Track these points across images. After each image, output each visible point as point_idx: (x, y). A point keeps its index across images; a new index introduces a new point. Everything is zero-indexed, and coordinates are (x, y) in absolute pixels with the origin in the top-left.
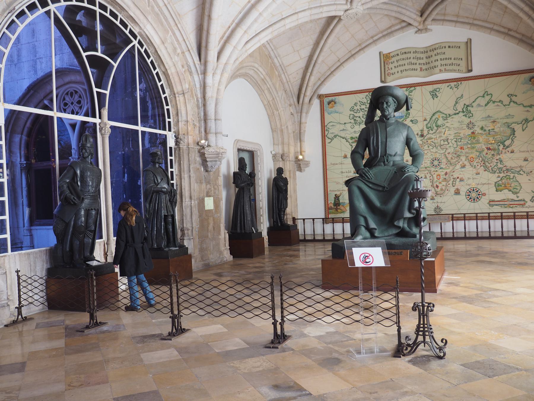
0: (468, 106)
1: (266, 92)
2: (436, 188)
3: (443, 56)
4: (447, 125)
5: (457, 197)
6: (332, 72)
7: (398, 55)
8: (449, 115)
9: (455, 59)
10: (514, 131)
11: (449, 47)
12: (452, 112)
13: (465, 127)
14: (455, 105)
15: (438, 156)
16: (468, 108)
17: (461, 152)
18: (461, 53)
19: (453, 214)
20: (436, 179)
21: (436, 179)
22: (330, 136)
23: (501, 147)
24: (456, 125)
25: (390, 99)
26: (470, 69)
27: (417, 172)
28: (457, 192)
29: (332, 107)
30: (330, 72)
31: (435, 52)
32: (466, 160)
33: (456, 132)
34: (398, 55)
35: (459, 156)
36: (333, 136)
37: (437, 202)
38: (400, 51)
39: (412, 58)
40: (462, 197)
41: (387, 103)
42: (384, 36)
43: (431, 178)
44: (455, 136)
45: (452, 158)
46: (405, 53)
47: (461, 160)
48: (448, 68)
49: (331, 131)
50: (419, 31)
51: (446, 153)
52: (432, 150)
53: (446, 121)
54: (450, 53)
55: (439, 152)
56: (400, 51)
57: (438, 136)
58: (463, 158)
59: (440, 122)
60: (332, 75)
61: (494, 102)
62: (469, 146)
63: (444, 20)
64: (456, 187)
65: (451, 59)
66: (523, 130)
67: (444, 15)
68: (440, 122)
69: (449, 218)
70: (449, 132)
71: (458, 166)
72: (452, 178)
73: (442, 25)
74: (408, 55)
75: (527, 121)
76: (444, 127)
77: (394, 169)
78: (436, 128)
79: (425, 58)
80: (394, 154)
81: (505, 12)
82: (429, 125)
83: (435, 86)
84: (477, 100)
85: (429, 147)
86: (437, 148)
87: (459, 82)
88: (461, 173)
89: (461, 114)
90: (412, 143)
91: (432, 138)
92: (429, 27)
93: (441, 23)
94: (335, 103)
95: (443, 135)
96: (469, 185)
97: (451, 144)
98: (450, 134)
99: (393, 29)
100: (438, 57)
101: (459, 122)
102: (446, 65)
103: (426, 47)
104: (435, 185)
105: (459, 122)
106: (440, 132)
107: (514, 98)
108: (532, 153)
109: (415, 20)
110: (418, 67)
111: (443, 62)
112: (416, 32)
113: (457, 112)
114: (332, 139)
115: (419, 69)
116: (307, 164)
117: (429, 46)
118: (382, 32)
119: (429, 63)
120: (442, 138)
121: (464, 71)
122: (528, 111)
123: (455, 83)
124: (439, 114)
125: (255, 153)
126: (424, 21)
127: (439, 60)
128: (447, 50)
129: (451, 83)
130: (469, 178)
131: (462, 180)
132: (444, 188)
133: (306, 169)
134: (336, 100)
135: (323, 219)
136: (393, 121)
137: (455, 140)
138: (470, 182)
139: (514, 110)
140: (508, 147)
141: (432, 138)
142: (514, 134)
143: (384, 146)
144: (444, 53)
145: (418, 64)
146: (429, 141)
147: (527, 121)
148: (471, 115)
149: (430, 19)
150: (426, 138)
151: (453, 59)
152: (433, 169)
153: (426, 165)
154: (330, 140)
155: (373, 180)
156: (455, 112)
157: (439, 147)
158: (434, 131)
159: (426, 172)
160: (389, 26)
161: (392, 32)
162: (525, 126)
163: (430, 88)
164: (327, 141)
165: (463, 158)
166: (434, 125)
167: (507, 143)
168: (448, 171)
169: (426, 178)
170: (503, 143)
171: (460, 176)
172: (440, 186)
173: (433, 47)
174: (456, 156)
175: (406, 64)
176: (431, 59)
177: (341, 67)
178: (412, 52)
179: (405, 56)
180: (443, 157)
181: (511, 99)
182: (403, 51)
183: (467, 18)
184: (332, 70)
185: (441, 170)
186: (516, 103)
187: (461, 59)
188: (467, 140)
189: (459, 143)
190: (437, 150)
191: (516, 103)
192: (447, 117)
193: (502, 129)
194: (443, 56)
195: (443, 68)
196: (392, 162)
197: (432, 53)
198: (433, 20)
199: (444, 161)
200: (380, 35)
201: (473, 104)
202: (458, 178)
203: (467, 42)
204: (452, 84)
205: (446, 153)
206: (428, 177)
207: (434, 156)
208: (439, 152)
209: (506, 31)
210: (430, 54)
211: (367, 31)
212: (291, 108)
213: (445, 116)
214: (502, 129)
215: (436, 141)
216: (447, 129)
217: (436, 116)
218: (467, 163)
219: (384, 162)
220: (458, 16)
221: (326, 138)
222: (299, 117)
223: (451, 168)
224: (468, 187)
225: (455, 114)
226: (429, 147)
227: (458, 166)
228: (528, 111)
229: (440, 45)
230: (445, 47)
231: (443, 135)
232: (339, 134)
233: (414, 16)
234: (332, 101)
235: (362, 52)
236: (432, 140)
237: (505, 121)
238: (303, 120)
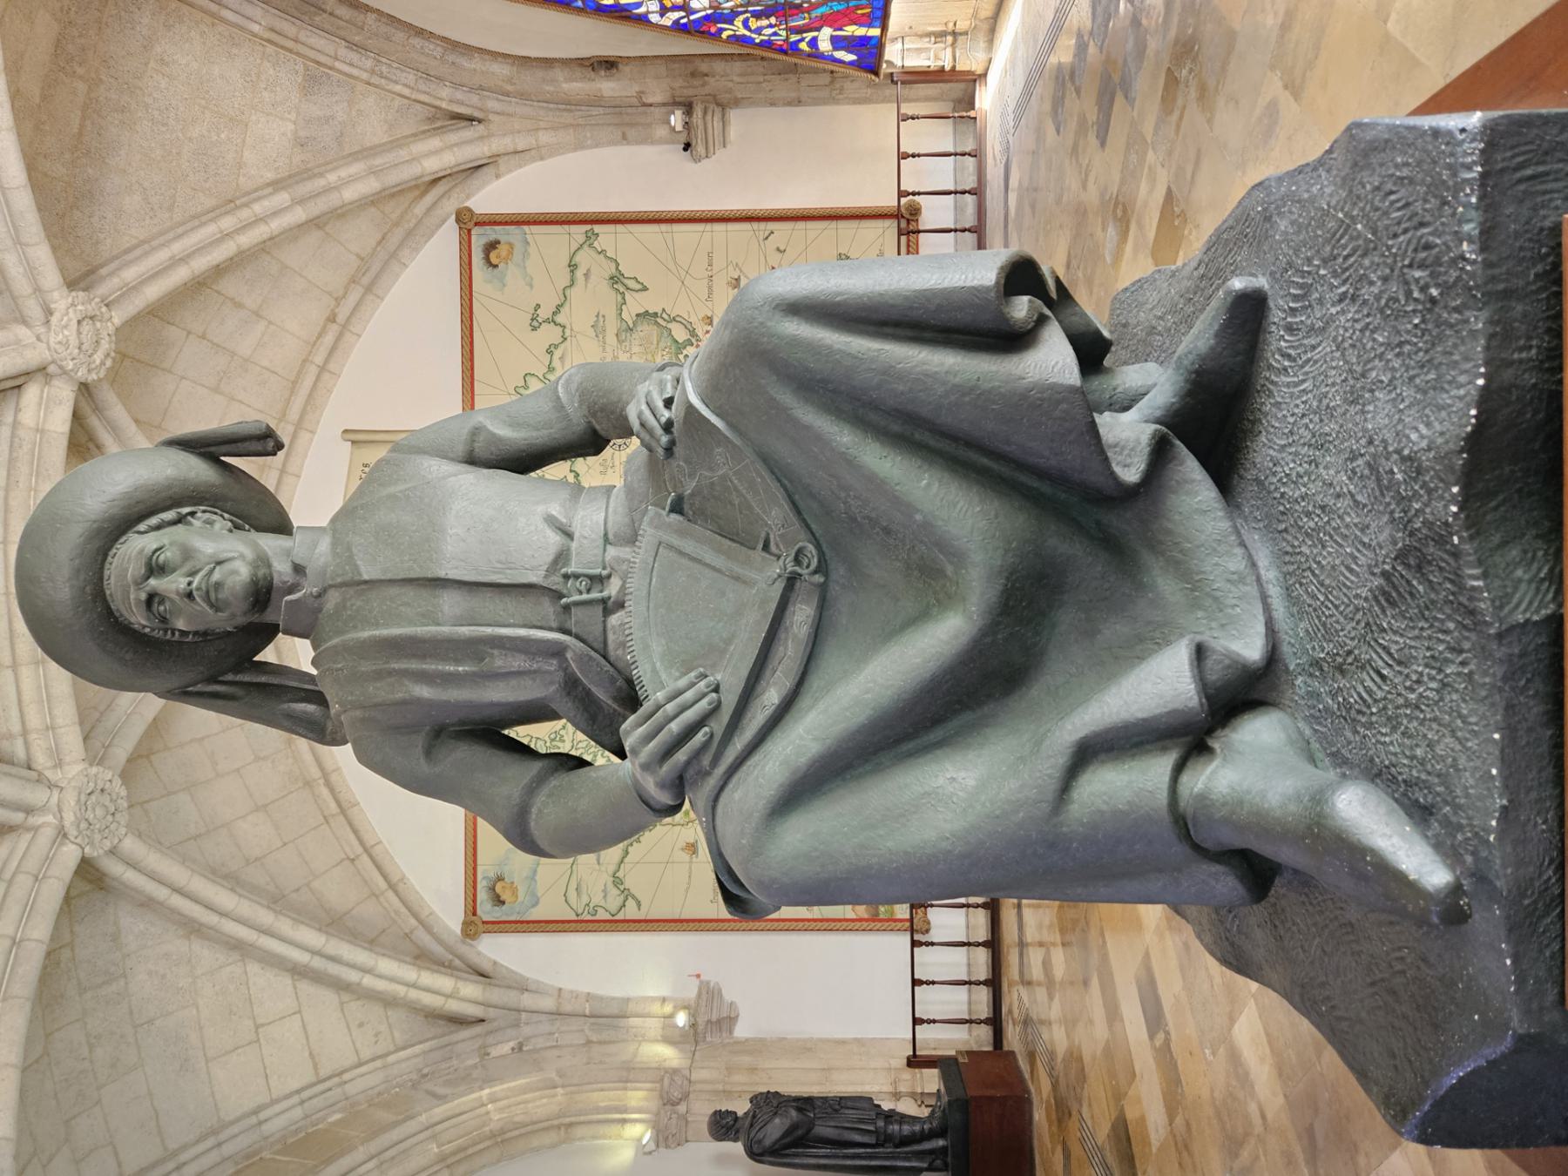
6: (392, 887)
10: (644, 315)
22: (613, 902)
23: (690, 351)
29: (514, 892)
30: (390, 894)
36: (616, 892)
49: (597, 899)
60: (401, 887)
61: (551, 369)
66: (645, 289)
75: (616, 279)
80: (554, 539)
81: (257, 314)
94: (500, 879)
107: (544, 313)
108: (715, 268)
114: (627, 894)
116: (709, 993)
122: (587, 275)
133: (729, 995)
134: (492, 875)
135: (914, 944)
139: (579, 315)
140: (693, 333)
142: (656, 314)
147: (616, 279)
154: (631, 903)
162: (632, 284)
164: (631, 912)
167: (680, 334)
170: (680, 347)
177: (377, 851)
181: (547, 321)
184: (383, 884)
186: (559, 308)
191: (559, 308)
193: (636, 349)
203: (353, 442)
209: (334, 330)
211: (258, 759)
212: (495, 1052)
214: (636, 349)
221: (620, 916)
222: (535, 1017)
228: (587, 275)
232: (612, 868)
234: (492, 889)
235: (334, 778)
237: (611, 338)
238: (548, 1003)
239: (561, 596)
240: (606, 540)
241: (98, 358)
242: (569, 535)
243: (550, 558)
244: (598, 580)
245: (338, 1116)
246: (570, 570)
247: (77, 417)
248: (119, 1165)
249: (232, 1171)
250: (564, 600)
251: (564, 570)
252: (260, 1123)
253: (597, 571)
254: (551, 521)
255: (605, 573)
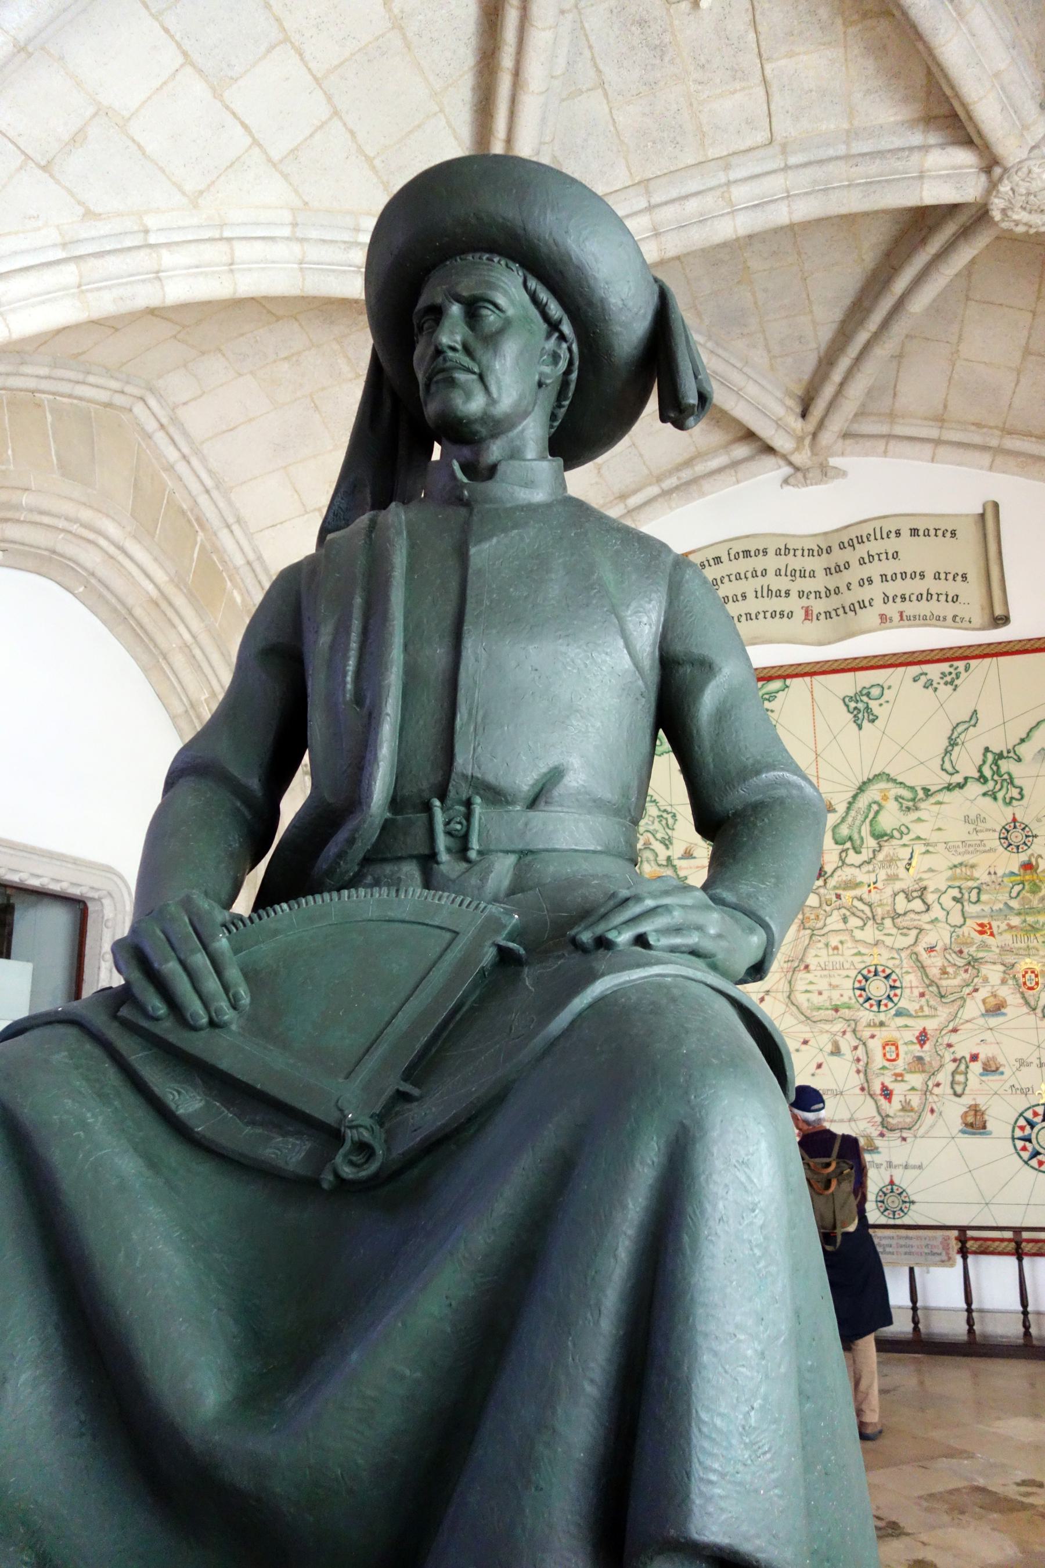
0: (1000, 756)
1: (179, 660)
2: (882, 1101)
3: (890, 567)
4: (917, 830)
5: (973, 1143)
7: (718, 560)
8: (926, 790)
9: (937, 576)
11: (914, 532)
12: (938, 780)
13: (992, 840)
14: (946, 752)
15: (882, 958)
16: (1005, 765)
17: (984, 946)
18: (963, 554)
19: (962, 1229)
20: (878, 1061)
21: (878, 1061)
24: (958, 832)
25: (510, 290)
26: (999, 611)
27: (757, 971)
28: (975, 1123)
31: (862, 550)
32: (1004, 982)
33: (957, 860)
34: (718, 560)
35: (973, 963)
37: (890, 1165)
38: (727, 546)
39: (771, 572)
40: (997, 1146)
41: (473, 308)
42: (666, 494)
43: (860, 1052)
44: (953, 878)
45: (944, 972)
46: (747, 553)
47: (986, 980)
48: (911, 608)
50: (799, 474)
51: (920, 949)
52: (859, 934)
53: (914, 815)
54: (916, 554)
55: (889, 940)
56: (727, 546)
57: (882, 875)
58: (993, 973)
59: (889, 819)
62: (1015, 921)
63: (889, 437)
64: (967, 1100)
65: (922, 576)
67: (892, 416)
68: (889, 819)
69: (946, 1248)
70: (929, 861)
71: (973, 1008)
72: (948, 1056)
73: (885, 453)
74: (757, 563)
76: (906, 839)
77: (493, 924)
78: (872, 843)
79: (820, 573)
80: (525, 781)
82: (844, 831)
83: (866, 678)
84: (1037, 734)
85: (845, 920)
86: (880, 926)
87: (961, 664)
88: (988, 1035)
89: (975, 789)
90: (708, 702)
91: (858, 885)
92: (833, 461)
93: (881, 444)
95: (902, 872)
96: (1025, 1092)
97: (936, 912)
98: (933, 869)
99: (700, 468)
100: (874, 570)
101: (967, 819)
102: (903, 598)
103: (826, 534)
104: (877, 1088)
105: (967, 819)
106: (891, 861)
109: (778, 424)
110: (793, 603)
111: (894, 588)
112: (786, 481)
113: (958, 779)
115: (800, 614)
117: (837, 530)
118: (659, 480)
119: (837, 591)
120: (898, 886)
121: (978, 619)
123: (945, 667)
124: (882, 785)
125: (91, 907)
126: (815, 435)
127: (876, 579)
128: (905, 544)
129: (925, 668)
130: (1022, 1063)
131: (991, 1069)
132: (915, 1101)
136: (539, 496)
137: (955, 893)
138: (1027, 1077)
141: (858, 885)
143: (430, 702)
144: (896, 555)
145: (794, 594)
146: (847, 895)
148: (1015, 793)
149: (837, 424)
150: (832, 882)
151: (929, 575)
152: (865, 1016)
153: (835, 994)
155: (233, 1051)
156: (947, 779)
157: (888, 922)
158: (866, 854)
159: (839, 1026)
160: (686, 456)
161: (695, 481)
163: (846, 683)
165: (993, 973)
166: (865, 830)
168: (931, 1025)
169: (836, 1051)
171: (984, 1053)
172: (899, 1090)
173: (853, 533)
174: (960, 962)
175: (751, 595)
176: (847, 576)
178: (771, 552)
179: (744, 565)
180: (907, 964)
182: (739, 547)
183: (978, 425)
185: (900, 1021)
187: (964, 577)
188: (1004, 897)
189: (971, 909)
190: (879, 936)
192: (915, 799)
194: (890, 567)
195: (892, 610)
196: (502, 870)
197: (848, 555)
198: (846, 435)
199: (911, 980)
200: (653, 490)
201: (1022, 750)
202: (974, 1058)
203: (982, 516)
204: (934, 670)
205: (920, 949)
206: (845, 1048)
207: (868, 960)
208: (889, 940)
210: (839, 556)
213: (907, 794)
215: (874, 897)
216: (919, 848)
217: (873, 793)
218: (1006, 992)
219: (428, 860)
220: (940, 420)
223: (944, 1013)
224: (1021, 1103)
225: (949, 788)
226: (845, 920)
227: (973, 1008)
229: (877, 524)
230: (898, 533)
231: (902, 872)
233: (779, 411)
236: (857, 892)
239: (442, 798)
240: (523, 853)
241: (1022, 216)
242: (533, 803)
243: (490, 778)
244: (462, 849)
245: (238, 599)
246: (478, 810)
247: (953, 209)
248: (184, 404)
249: (185, 507)
250: (437, 803)
251: (478, 800)
252: (228, 527)
253: (475, 844)
254: (555, 775)
255: (473, 855)
